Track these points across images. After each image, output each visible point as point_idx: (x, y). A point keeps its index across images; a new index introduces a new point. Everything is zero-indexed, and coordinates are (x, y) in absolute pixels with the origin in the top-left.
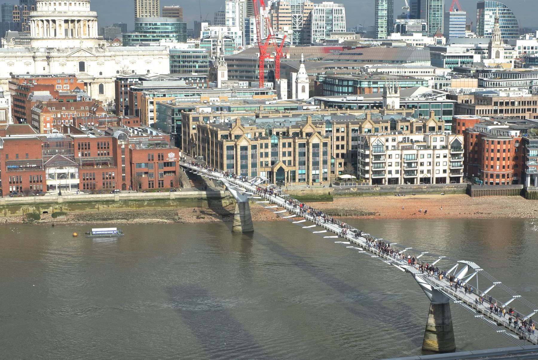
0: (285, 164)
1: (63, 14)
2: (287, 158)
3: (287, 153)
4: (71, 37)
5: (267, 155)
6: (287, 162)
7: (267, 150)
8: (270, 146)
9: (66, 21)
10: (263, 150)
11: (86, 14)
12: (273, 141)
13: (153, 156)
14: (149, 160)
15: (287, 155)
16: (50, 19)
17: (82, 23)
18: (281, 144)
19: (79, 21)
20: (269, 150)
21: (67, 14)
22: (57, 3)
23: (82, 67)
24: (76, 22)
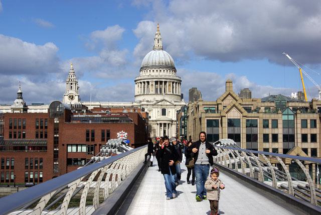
0: (307, 154)
1: (155, 77)
2: (309, 145)
3: (309, 136)
4: (159, 93)
5: (275, 138)
6: (309, 151)
7: (276, 131)
8: (280, 125)
9: (156, 83)
10: (269, 131)
11: (171, 77)
12: (285, 117)
13: (93, 135)
14: (88, 140)
15: (309, 140)
16: (145, 81)
17: (167, 83)
18: (299, 121)
19: (165, 82)
20: (280, 131)
21: (157, 77)
22: (152, 70)
23: (164, 112)
24: (163, 83)
